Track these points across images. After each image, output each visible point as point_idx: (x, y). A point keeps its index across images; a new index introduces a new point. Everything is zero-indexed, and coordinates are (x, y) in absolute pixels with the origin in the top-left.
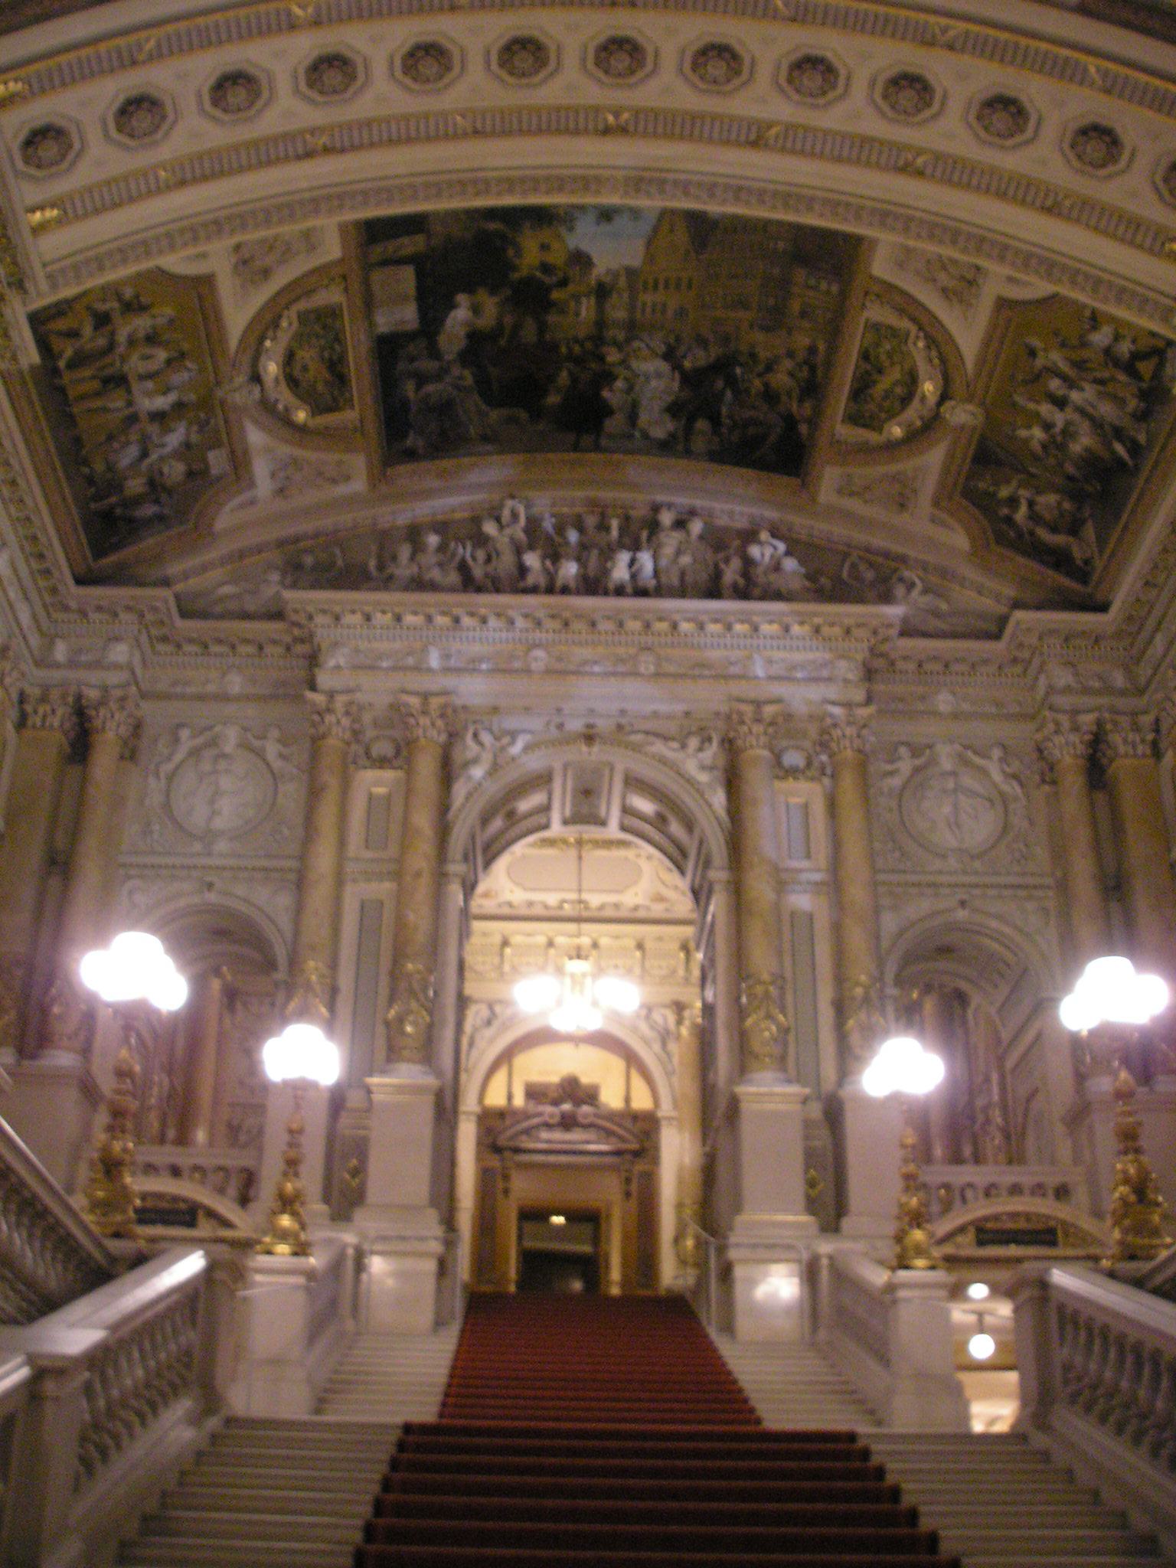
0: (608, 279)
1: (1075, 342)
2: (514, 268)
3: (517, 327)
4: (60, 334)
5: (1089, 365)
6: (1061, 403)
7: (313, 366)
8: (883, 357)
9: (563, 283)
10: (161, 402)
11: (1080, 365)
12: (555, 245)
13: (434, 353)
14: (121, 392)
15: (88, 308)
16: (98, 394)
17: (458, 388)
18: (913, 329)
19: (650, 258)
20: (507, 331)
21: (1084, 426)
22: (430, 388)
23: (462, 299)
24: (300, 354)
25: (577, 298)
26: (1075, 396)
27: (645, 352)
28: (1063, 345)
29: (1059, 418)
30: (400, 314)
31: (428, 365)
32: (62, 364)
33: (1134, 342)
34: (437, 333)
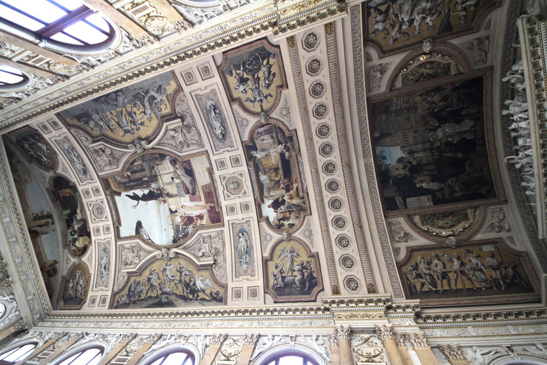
0: (407, 153)
1: (386, 32)
2: (405, 175)
3: (428, 170)
4: (422, 288)
5: (392, 23)
6: (411, 21)
7: (445, 221)
8: (416, 76)
9: (410, 163)
10: (456, 264)
11: (393, 26)
12: (396, 167)
13: (442, 189)
14: (449, 274)
15: (414, 279)
16: (449, 281)
17: (456, 182)
18: (401, 74)
19: (397, 144)
20: (430, 173)
21: (418, 8)
22: (457, 189)
23: (418, 186)
24: (440, 225)
25: (415, 158)
26: (406, 19)
27: (434, 136)
28: (388, 34)
29: (418, 18)
30: (426, 200)
31: (446, 191)
32: (434, 289)
33: (376, 17)
34: (433, 190)
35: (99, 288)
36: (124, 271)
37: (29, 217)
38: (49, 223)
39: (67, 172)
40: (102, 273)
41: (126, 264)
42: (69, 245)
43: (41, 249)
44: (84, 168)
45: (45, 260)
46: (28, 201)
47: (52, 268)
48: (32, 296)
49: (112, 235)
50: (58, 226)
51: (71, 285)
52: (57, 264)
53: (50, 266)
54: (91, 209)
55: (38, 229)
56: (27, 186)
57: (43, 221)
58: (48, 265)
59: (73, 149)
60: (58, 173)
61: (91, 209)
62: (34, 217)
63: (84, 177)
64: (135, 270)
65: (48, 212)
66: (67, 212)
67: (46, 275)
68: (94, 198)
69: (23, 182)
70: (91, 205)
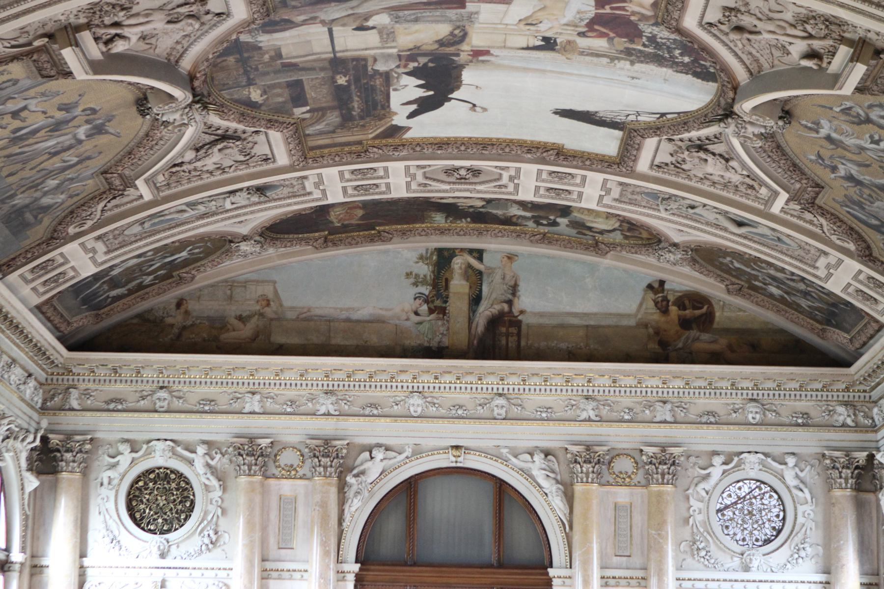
37: (426, 325)
38: (470, 266)
42: (597, 242)
43: (575, 321)
45: (632, 322)
46: (356, 316)
47: (673, 309)
48: (752, 407)
49: (596, 178)
50: (495, 245)
51: (774, 290)
52: (666, 286)
53: (665, 311)
54: (447, 187)
55: (485, 310)
56: (287, 303)
57: (459, 285)
58: (655, 316)
62: (431, 311)
65: (421, 258)
66: (439, 219)
67: (694, 333)
69: (269, 312)
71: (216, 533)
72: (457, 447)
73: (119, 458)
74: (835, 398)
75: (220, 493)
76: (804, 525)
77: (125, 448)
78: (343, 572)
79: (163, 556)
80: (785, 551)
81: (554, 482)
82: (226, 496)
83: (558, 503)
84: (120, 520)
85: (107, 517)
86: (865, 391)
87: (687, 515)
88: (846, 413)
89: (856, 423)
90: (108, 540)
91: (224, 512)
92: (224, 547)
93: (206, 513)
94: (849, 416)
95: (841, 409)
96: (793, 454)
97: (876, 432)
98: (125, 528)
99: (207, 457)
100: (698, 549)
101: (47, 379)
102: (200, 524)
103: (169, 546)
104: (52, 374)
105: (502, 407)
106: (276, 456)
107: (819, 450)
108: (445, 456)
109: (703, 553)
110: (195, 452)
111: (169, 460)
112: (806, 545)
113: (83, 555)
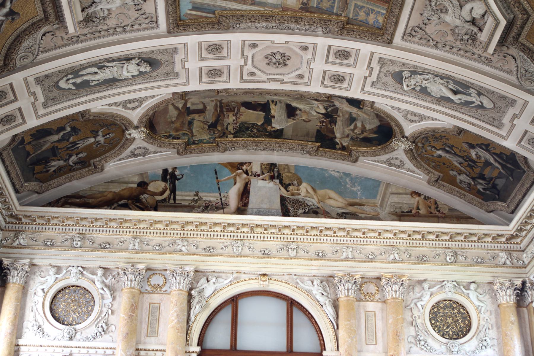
35: (506, 120)
36: (491, 49)
39: (140, 101)
40: (468, 103)
41: (473, 38)
44: (134, 62)
59: (75, 72)
60: (140, 121)
61: (264, 77)
63: (163, 70)
64: (503, 23)
68: (234, 62)
70: (253, 74)
71: (107, 324)
72: (264, 275)
73: (47, 277)
74: (499, 248)
75: (111, 300)
76: (484, 326)
77: (52, 271)
78: (189, 352)
79: (71, 339)
80: (474, 343)
81: (326, 298)
82: (114, 303)
83: (330, 310)
84: (46, 318)
85: (37, 313)
86: (517, 243)
87: (412, 320)
88: (506, 257)
89: (513, 264)
90: (35, 328)
91: (112, 313)
92: (111, 334)
93: (101, 312)
94: (508, 258)
95: (503, 255)
96: (474, 282)
97: (525, 267)
98: (48, 321)
99: (103, 277)
100: (419, 340)
101: (5, 227)
102: (97, 319)
103: (76, 333)
104: (9, 223)
105: (294, 249)
106: (148, 279)
107: (490, 279)
108: (257, 281)
109: (423, 343)
110: (97, 275)
111: (79, 280)
112: (486, 338)
113: (19, 336)
